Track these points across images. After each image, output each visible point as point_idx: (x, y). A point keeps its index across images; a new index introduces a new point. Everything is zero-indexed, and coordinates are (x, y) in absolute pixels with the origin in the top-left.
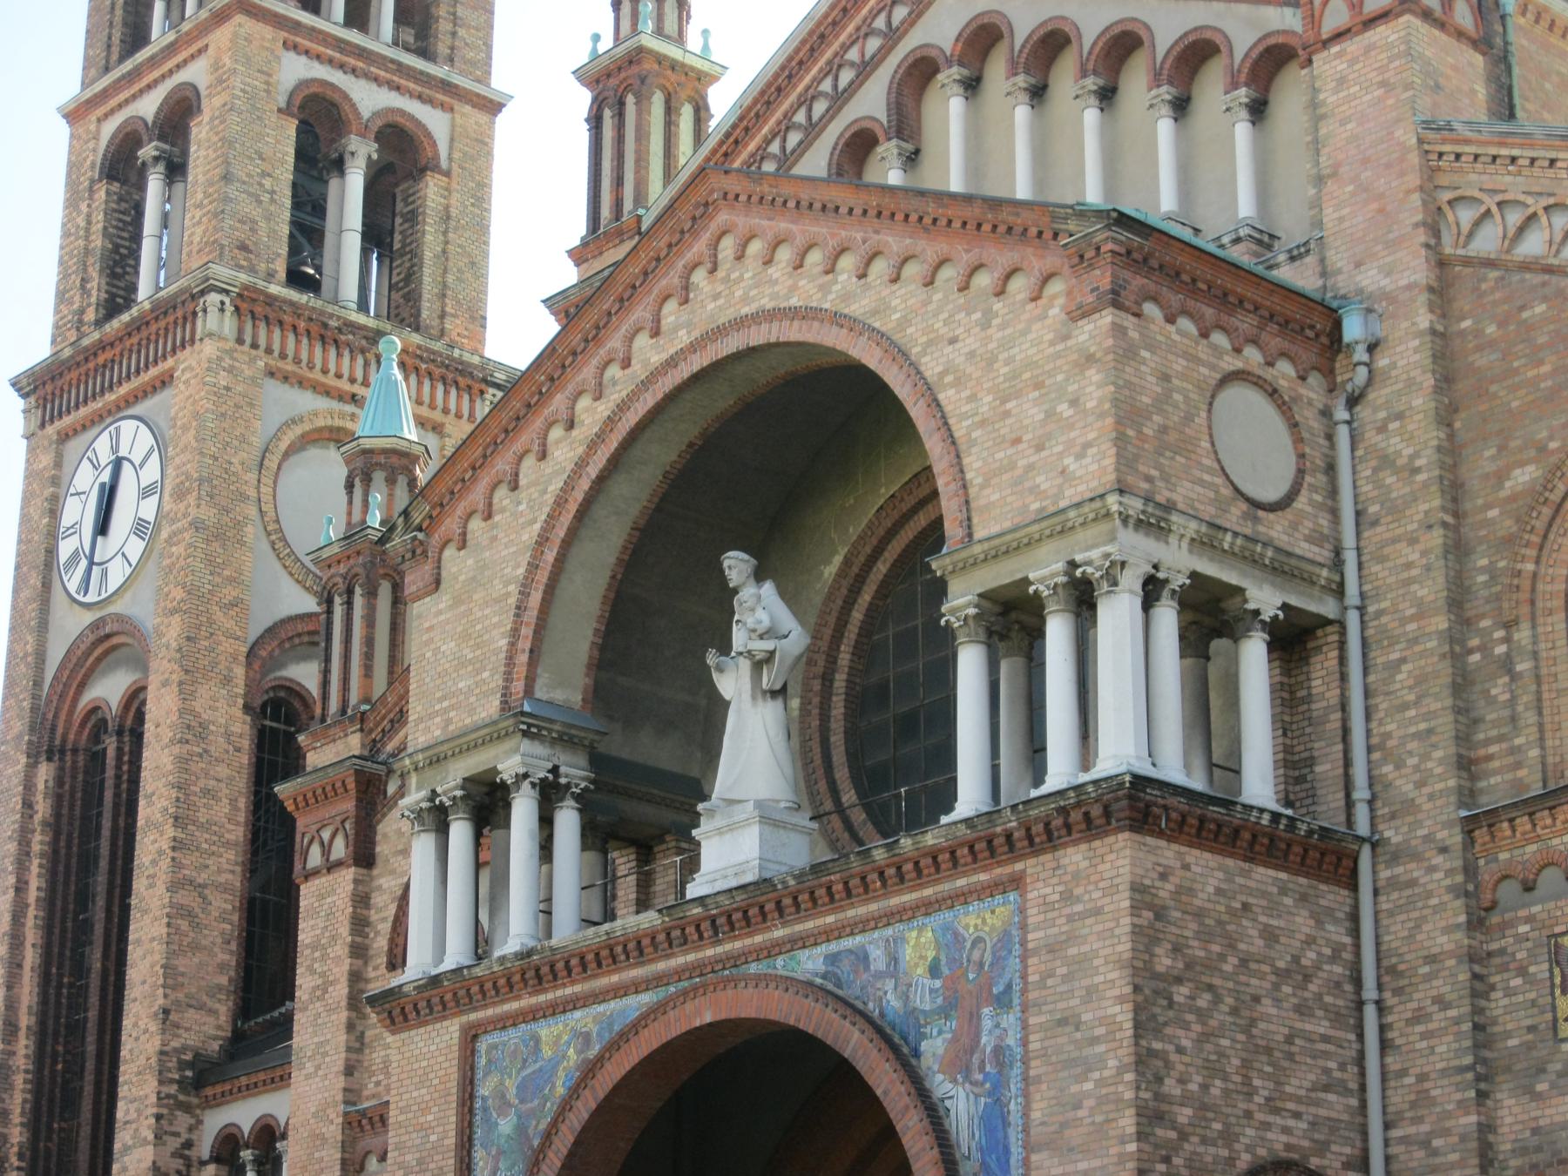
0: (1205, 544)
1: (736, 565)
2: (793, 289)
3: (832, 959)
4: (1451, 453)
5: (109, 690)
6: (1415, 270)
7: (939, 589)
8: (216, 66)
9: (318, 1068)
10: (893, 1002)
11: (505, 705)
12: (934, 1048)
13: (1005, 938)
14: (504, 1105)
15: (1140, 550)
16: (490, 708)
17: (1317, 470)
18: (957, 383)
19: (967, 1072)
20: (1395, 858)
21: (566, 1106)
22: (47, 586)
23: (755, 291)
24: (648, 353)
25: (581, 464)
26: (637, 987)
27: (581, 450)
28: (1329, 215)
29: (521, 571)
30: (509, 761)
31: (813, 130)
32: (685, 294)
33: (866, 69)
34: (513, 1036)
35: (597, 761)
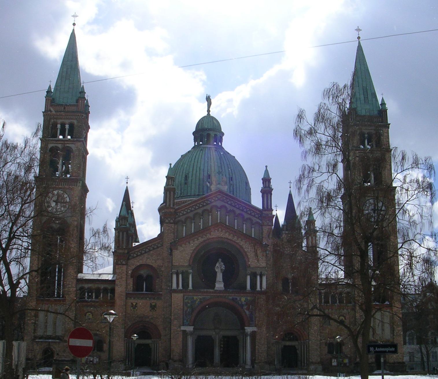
1: (220, 260)
3: (233, 298)
9: (121, 287)
10: (240, 303)
11: (189, 265)
12: (245, 307)
14: (189, 303)
19: (248, 310)
27: (199, 243)
29: (191, 252)
31: (199, 207)
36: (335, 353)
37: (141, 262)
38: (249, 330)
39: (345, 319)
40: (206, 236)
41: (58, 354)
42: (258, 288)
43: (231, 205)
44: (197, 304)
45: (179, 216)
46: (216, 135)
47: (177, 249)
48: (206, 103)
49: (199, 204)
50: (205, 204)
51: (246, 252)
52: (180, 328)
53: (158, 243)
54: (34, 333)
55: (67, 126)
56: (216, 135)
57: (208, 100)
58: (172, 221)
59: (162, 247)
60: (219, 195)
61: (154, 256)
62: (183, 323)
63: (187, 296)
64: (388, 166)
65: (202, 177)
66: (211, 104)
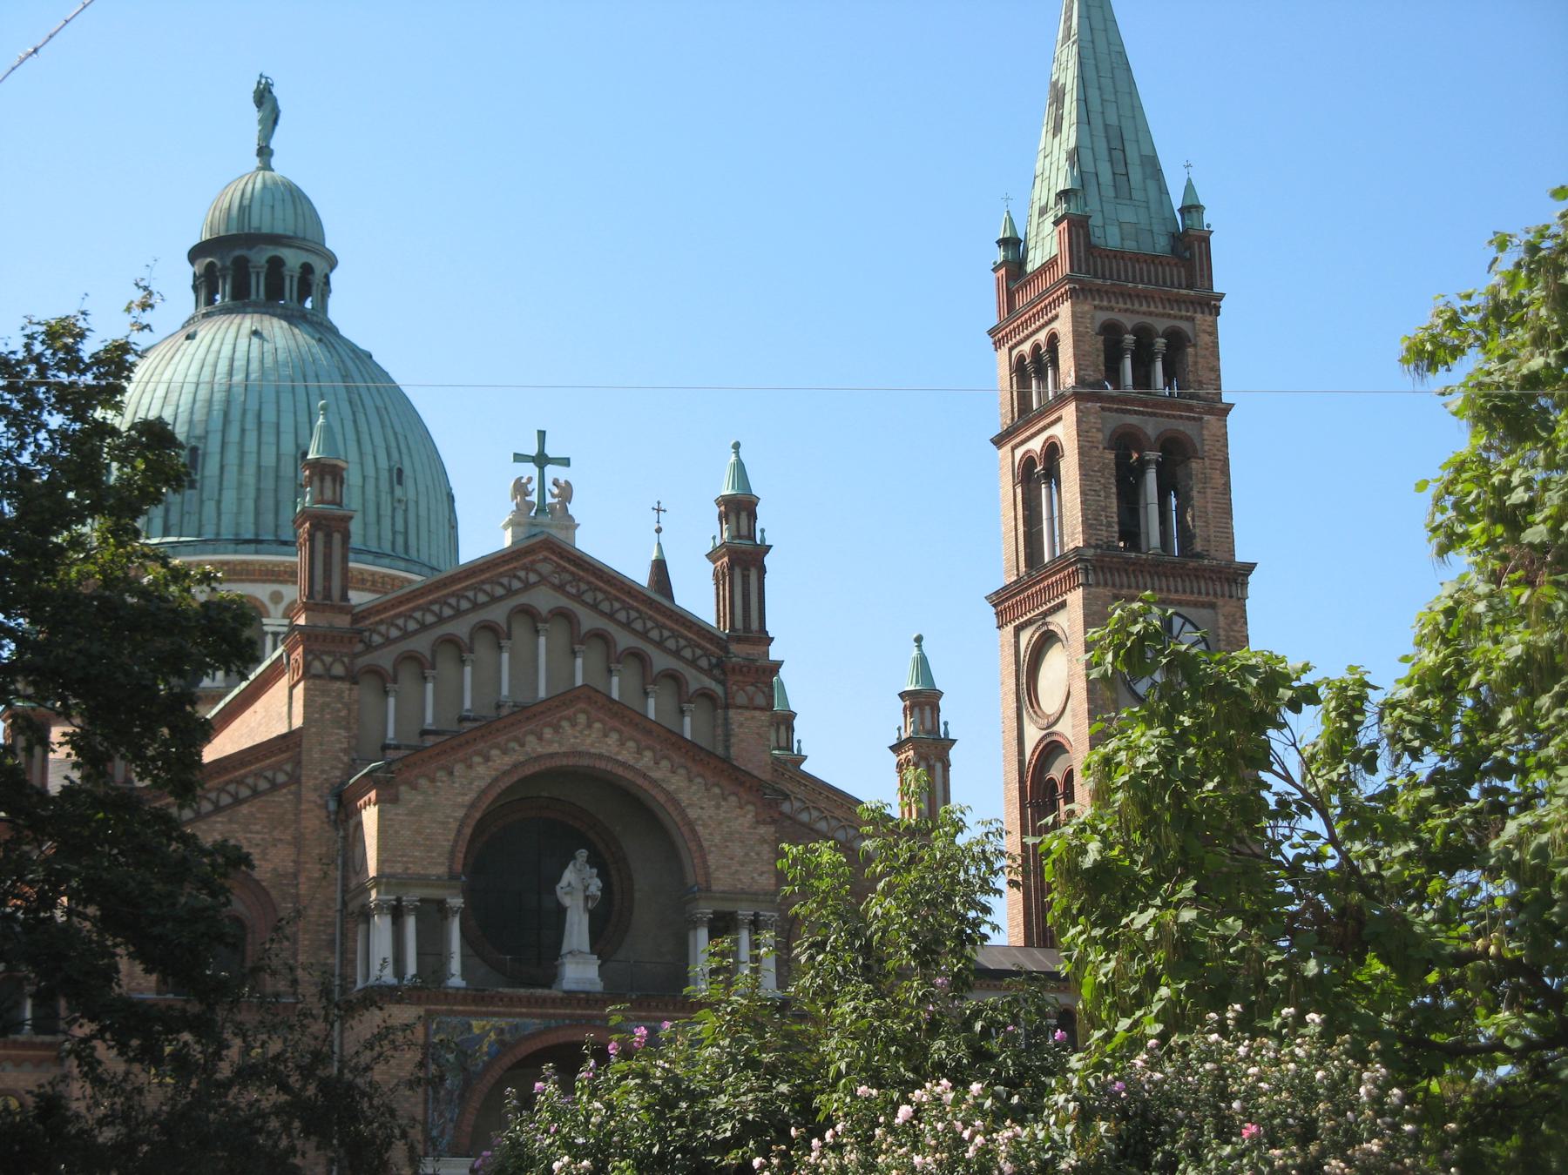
1: (582, 854)
2: (618, 753)
11: (452, 876)
16: (441, 870)
18: (705, 826)
24: (533, 746)
25: (496, 780)
29: (460, 813)
31: (459, 613)
32: (557, 728)
33: (494, 599)
34: (455, 1021)
40: (522, 745)
44: (488, 1054)
45: (369, 648)
46: (307, 269)
48: (252, 116)
49: (459, 596)
50: (482, 598)
51: (690, 824)
53: (277, 768)
56: (307, 269)
57: (264, 96)
58: (338, 670)
59: (293, 788)
60: (545, 559)
61: (258, 827)
63: (444, 1019)
65: (269, 460)
66: (275, 122)
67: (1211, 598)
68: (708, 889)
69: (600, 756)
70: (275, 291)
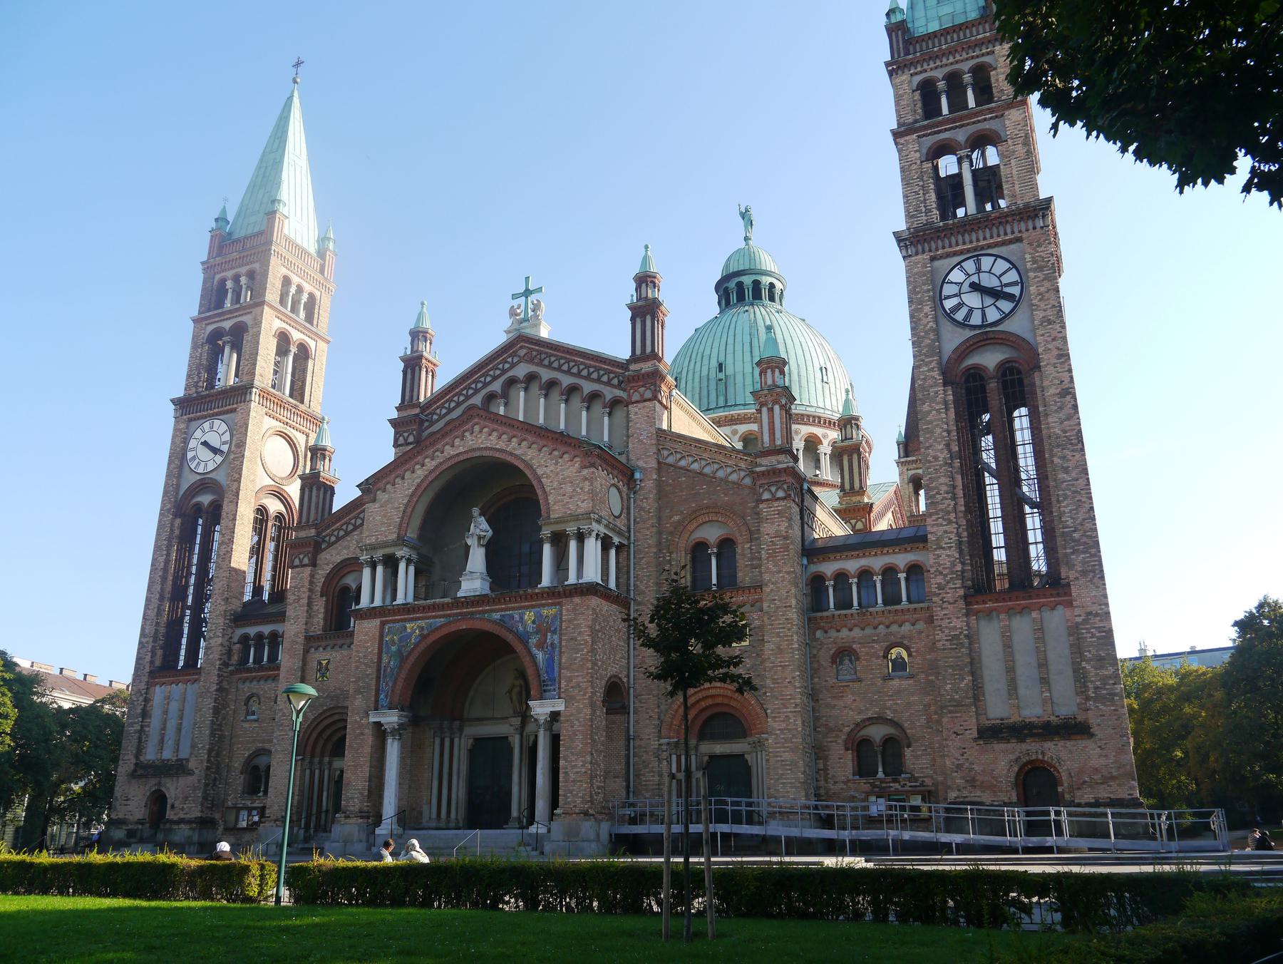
0: (607, 526)
4: (660, 509)
5: (206, 499)
6: (654, 464)
7: (540, 529)
8: (255, 319)
10: (521, 628)
11: (399, 537)
12: (533, 641)
13: (555, 616)
15: (595, 526)
16: (395, 536)
17: (626, 508)
20: (639, 604)
21: (416, 645)
22: (181, 465)
23: (480, 441)
24: (449, 451)
25: (426, 477)
26: (440, 617)
28: (630, 445)
30: (401, 552)
31: (477, 391)
33: (495, 378)
34: (397, 625)
35: (418, 554)
36: (880, 774)
37: (345, 554)
38: (541, 709)
39: (910, 655)
41: (173, 807)
42: (572, 579)
43: (550, 366)
45: (432, 423)
46: (757, 284)
47: (374, 501)
49: (476, 382)
51: (539, 479)
52: (367, 716)
54: (137, 757)
55: (243, 280)
57: (745, 215)
60: (521, 347)
62: (377, 701)
64: (1019, 148)
65: (705, 373)
67: (1017, 234)
68: (549, 517)
69: (486, 449)
70: (741, 298)
